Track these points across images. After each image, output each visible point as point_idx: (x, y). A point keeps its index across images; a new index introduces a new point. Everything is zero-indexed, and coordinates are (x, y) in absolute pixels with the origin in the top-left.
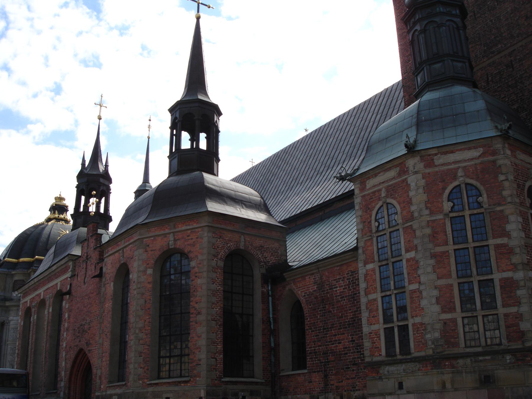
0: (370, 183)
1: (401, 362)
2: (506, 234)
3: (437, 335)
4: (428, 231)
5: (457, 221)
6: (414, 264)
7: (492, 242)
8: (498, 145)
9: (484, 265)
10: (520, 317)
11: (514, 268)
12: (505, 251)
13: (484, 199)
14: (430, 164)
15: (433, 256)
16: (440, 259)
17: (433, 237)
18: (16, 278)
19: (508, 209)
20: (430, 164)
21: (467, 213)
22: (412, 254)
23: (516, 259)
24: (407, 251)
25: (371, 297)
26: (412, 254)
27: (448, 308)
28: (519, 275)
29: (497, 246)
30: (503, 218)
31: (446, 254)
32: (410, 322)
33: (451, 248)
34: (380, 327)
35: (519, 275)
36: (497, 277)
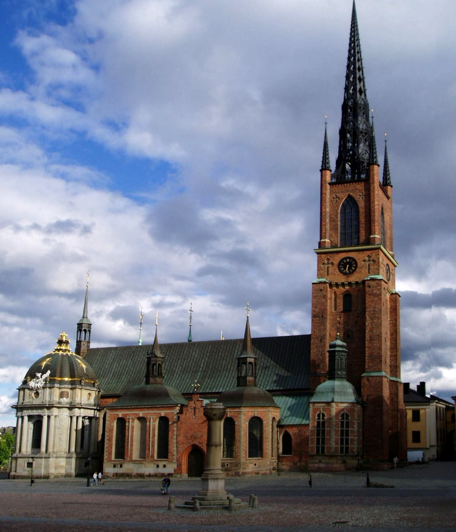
0: (317, 405)
1: (321, 456)
2: (353, 428)
3: (333, 450)
4: (334, 424)
5: (342, 423)
6: (329, 432)
7: (350, 429)
8: (355, 405)
9: (347, 435)
10: (354, 448)
11: (354, 436)
12: (353, 432)
13: (350, 418)
14: (337, 406)
15: (335, 430)
16: (337, 431)
17: (336, 425)
18: (63, 390)
19: (355, 422)
20: (337, 406)
21: (345, 421)
22: (329, 429)
23: (355, 434)
24: (327, 427)
25: (313, 437)
26: (329, 429)
27: (337, 444)
28: (355, 438)
29: (351, 430)
30: (354, 424)
31: (338, 430)
32: (326, 446)
33: (340, 429)
34: (315, 445)
35: (355, 438)
36: (350, 438)
